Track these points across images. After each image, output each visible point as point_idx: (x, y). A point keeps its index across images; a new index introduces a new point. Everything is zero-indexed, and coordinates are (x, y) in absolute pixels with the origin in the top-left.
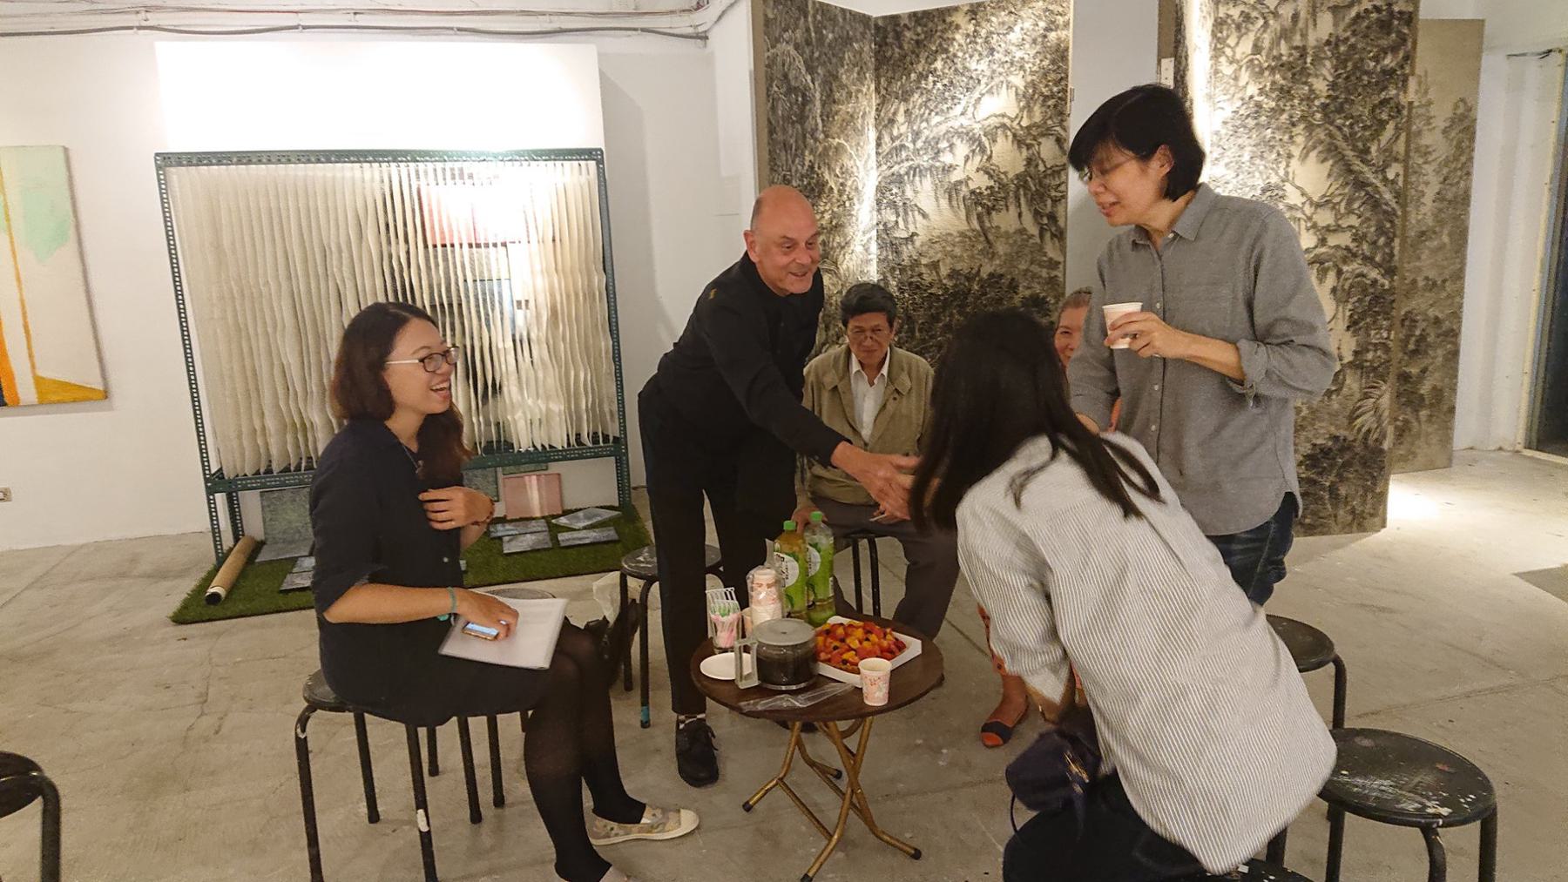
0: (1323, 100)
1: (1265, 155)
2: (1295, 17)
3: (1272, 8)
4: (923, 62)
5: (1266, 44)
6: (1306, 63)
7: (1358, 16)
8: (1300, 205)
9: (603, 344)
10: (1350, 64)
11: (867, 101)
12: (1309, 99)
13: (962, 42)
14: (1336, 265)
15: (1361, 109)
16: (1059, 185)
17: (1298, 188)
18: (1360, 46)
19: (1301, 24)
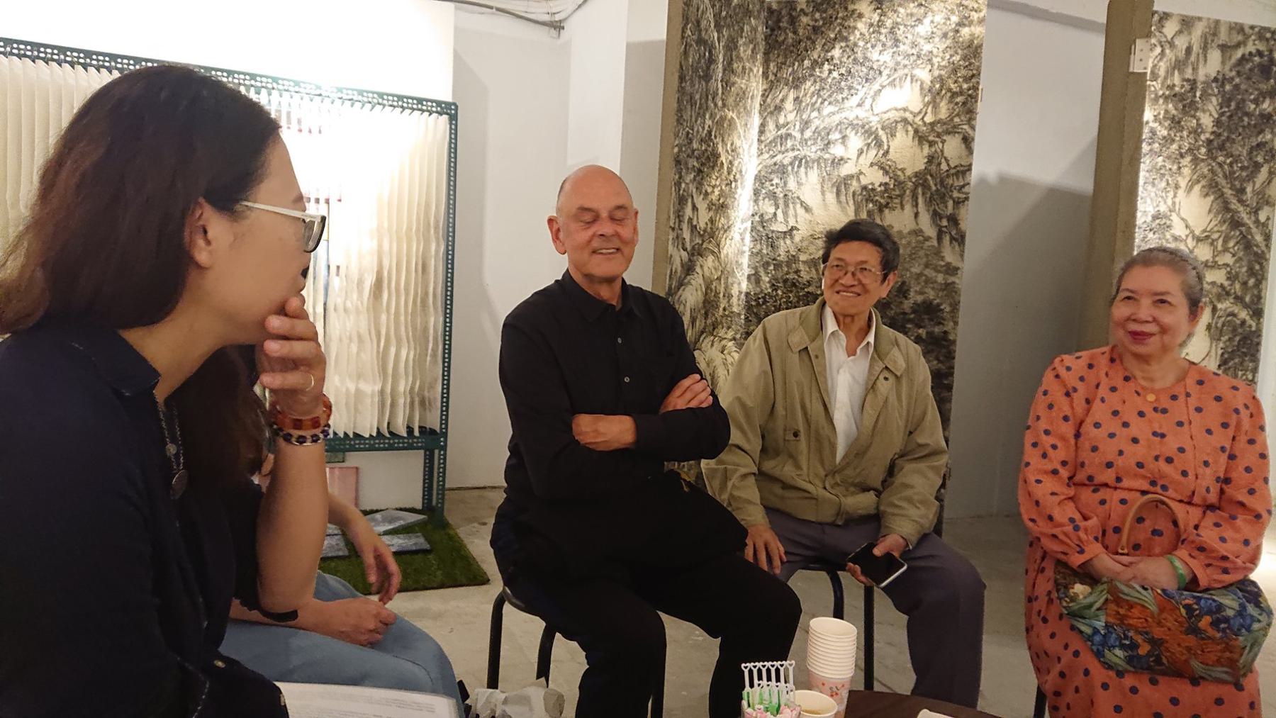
0: (1208, 135)
1: (1156, 182)
2: (1189, 50)
3: (1169, 38)
4: (819, 49)
5: (1162, 72)
6: (1195, 96)
7: (1243, 55)
8: (1184, 238)
9: (432, 320)
10: (1233, 105)
11: (755, 85)
12: (1196, 132)
13: (864, 30)
14: (1211, 302)
15: (1240, 149)
16: (963, 186)
17: (1183, 219)
18: (1243, 87)
19: (1193, 58)
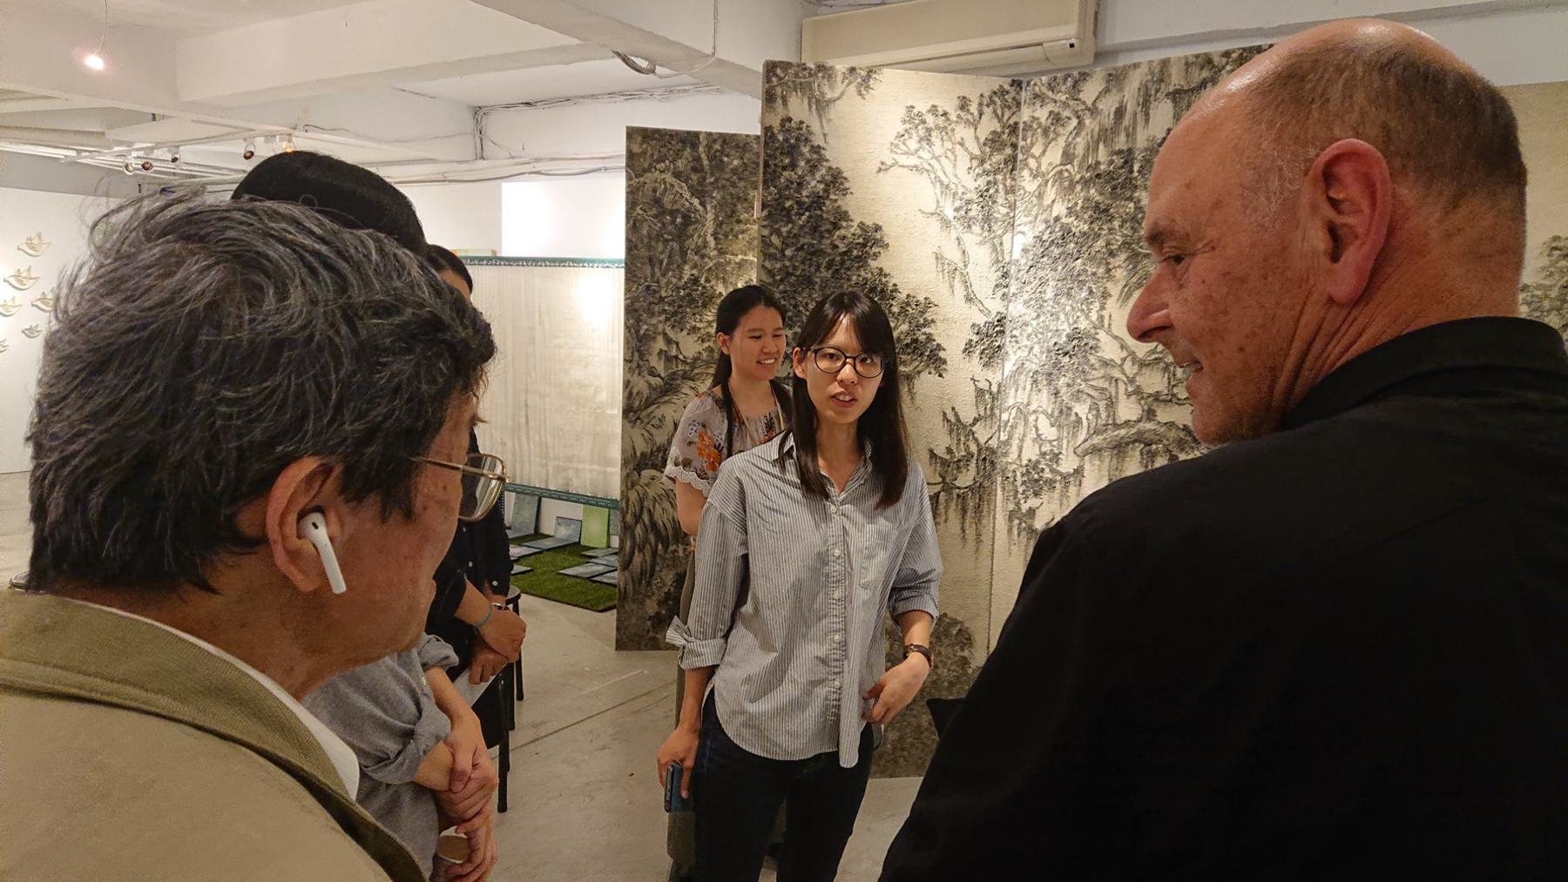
1: (1073, 292)
2: (1120, 113)
3: (1089, 103)
5: (1080, 151)
6: (1131, 172)
8: (1119, 362)
12: (1135, 220)
17: (1116, 338)
19: (1126, 121)
